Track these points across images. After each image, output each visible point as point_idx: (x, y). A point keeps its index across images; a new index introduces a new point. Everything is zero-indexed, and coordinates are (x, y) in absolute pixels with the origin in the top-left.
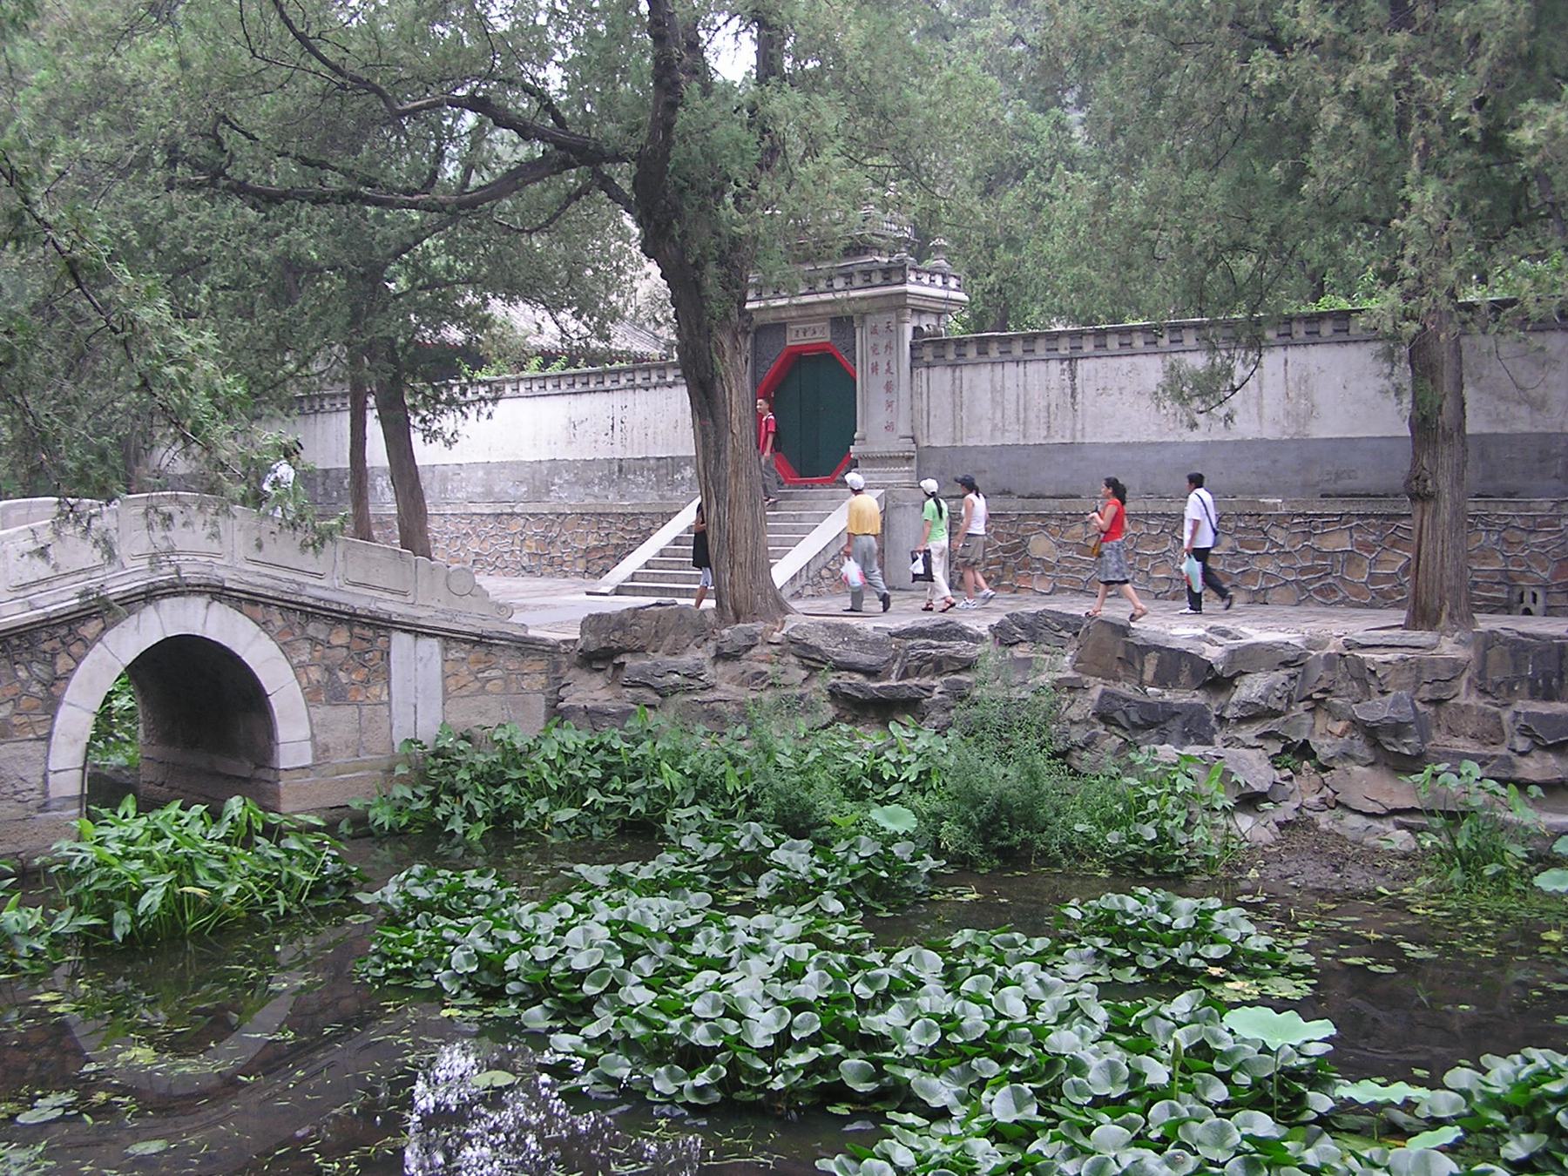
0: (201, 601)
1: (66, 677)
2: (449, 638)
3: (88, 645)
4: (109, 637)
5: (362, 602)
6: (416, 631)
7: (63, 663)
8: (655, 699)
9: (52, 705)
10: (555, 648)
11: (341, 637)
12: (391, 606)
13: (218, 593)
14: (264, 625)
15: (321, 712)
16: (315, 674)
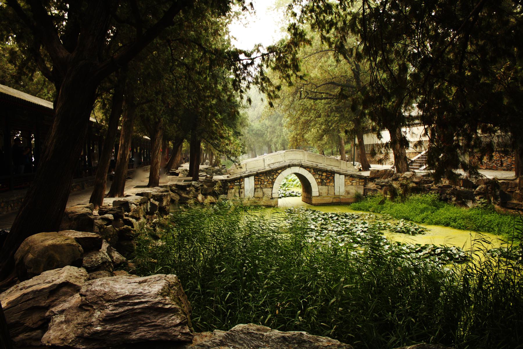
0: (298, 167)
1: (275, 179)
2: (346, 175)
3: (279, 174)
4: (283, 173)
5: (329, 168)
6: (340, 174)
7: (275, 176)
8: (380, 187)
9: (273, 183)
10: (366, 177)
11: (324, 174)
12: (335, 169)
13: (301, 166)
14: (310, 172)
15: (320, 187)
16: (319, 180)
